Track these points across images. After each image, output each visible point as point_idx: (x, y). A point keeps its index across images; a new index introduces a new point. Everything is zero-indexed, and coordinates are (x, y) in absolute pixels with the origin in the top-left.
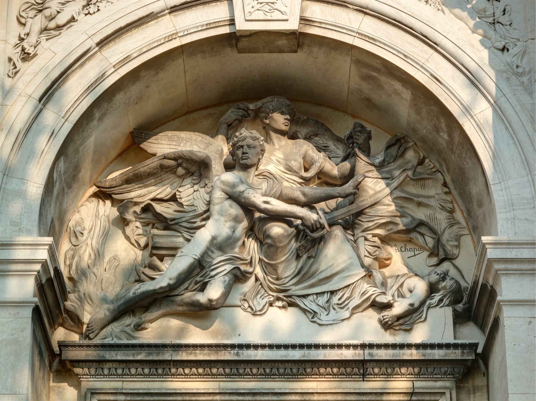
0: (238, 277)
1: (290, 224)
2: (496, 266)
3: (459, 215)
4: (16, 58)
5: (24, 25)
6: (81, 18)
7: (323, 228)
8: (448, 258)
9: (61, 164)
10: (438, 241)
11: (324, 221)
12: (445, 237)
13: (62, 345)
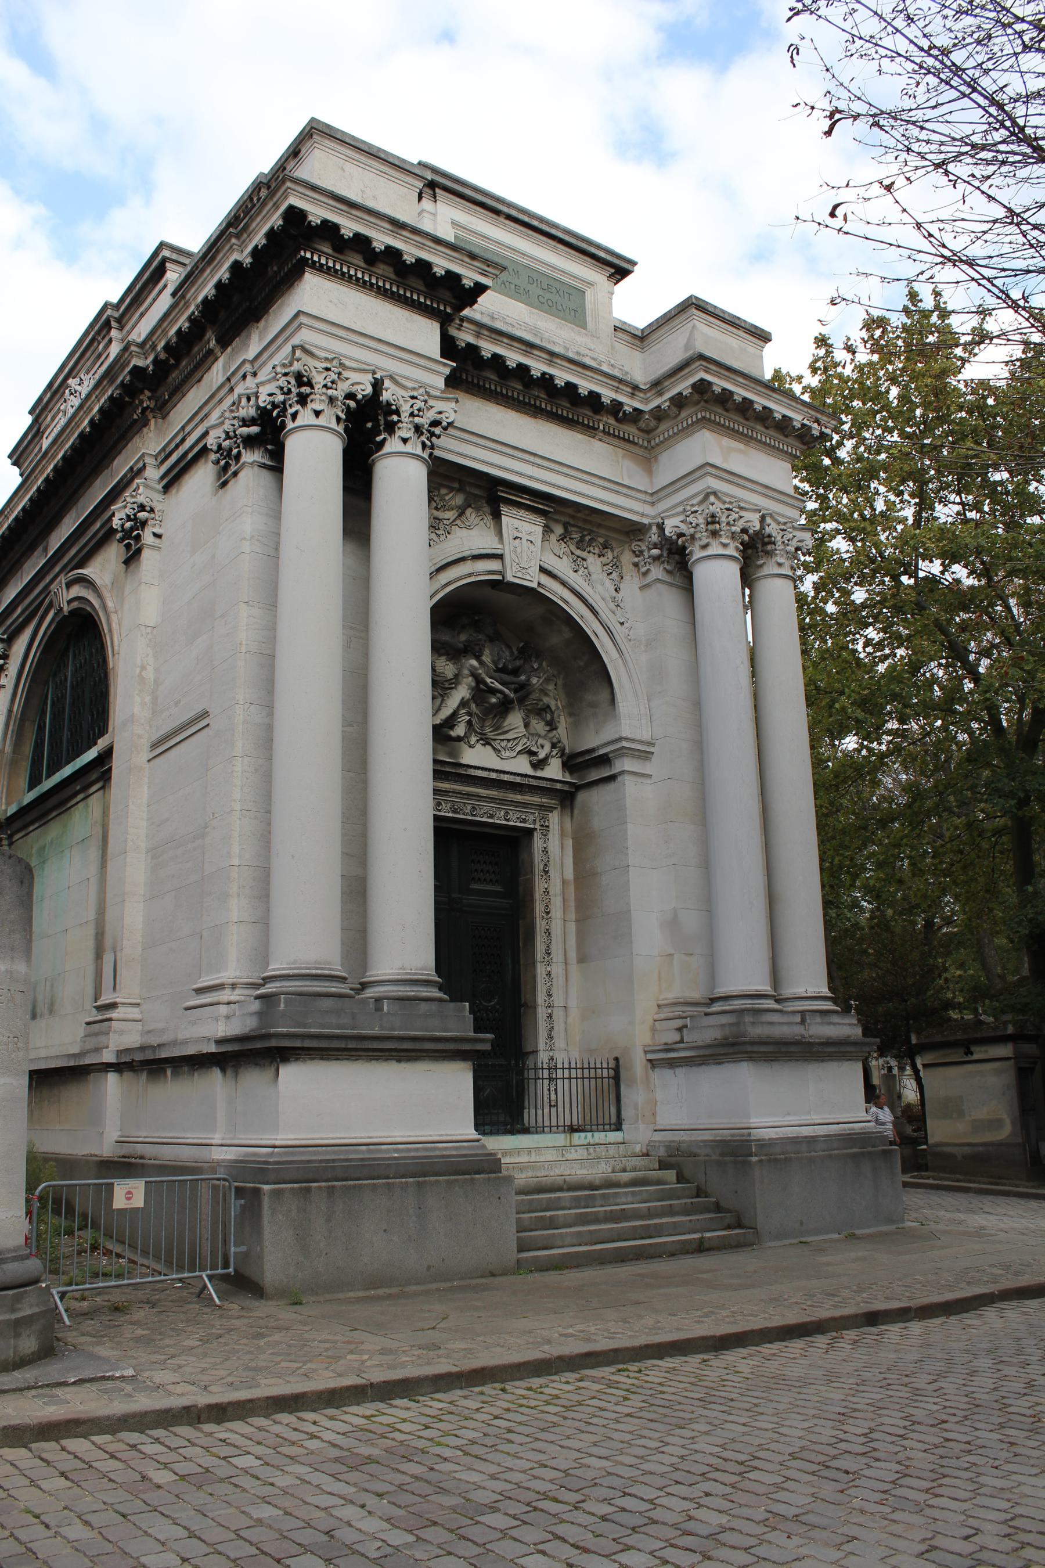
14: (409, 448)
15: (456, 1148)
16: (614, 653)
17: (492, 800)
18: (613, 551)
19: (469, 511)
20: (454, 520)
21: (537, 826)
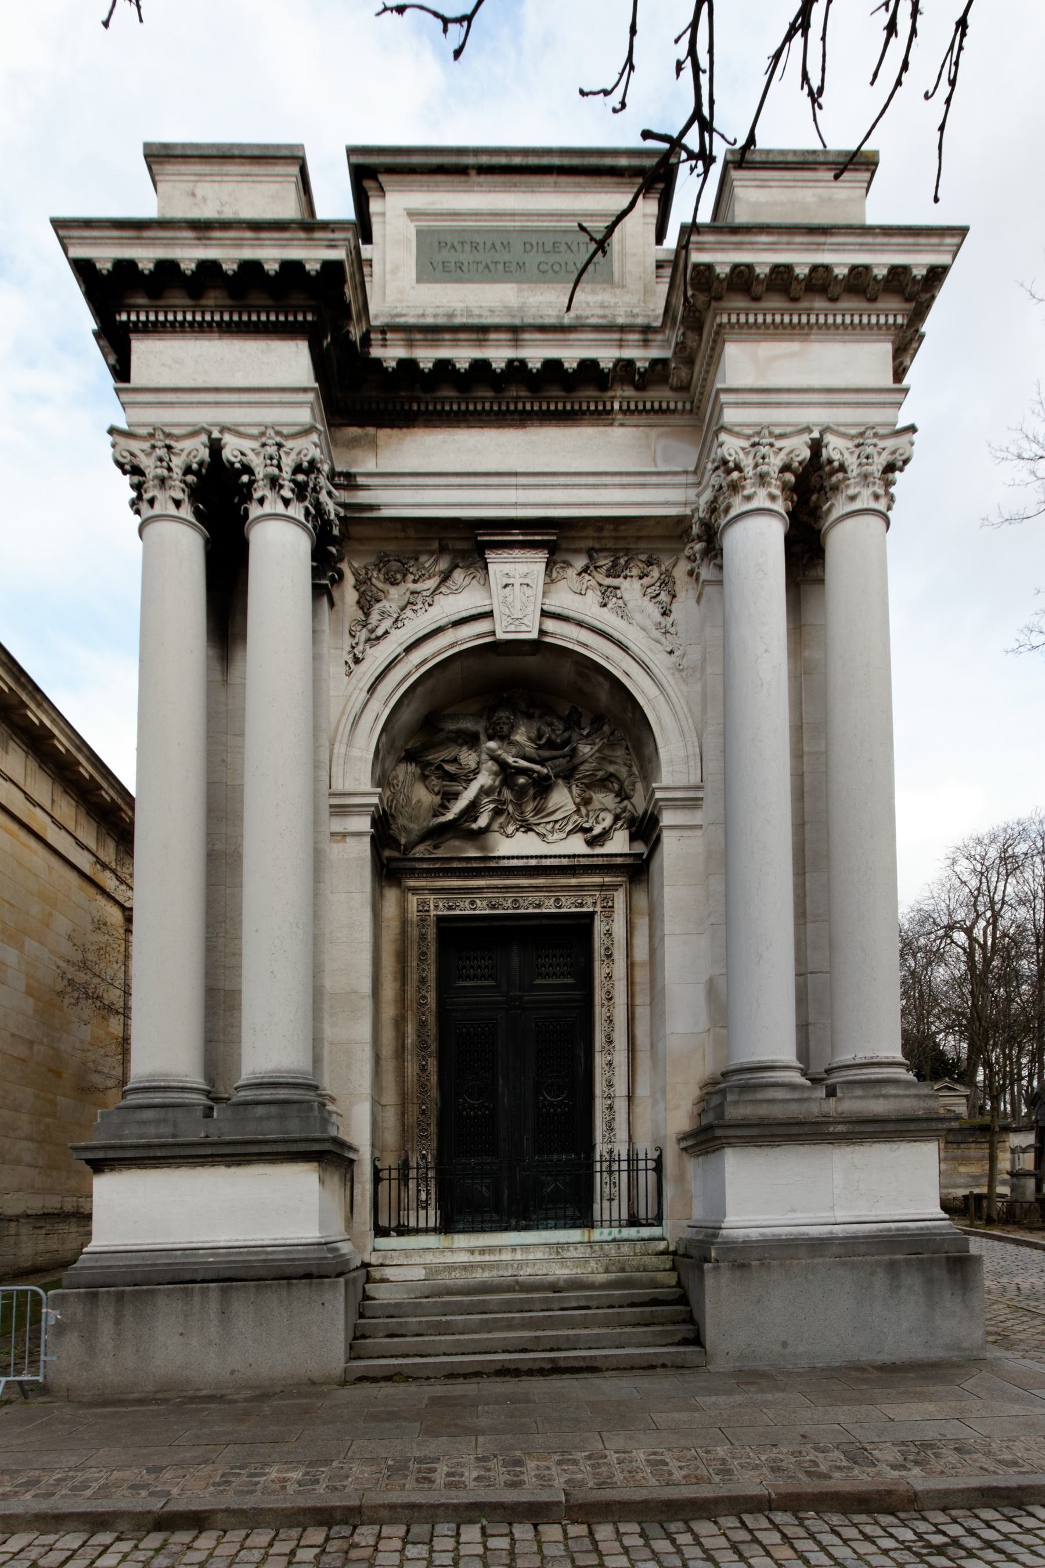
0: (497, 813)
1: (530, 776)
2: (661, 803)
3: (635, 770)
4: (350, 662)
5: (354, 637)
6: (393, 631)
7: (550, 778)
8: (628, 797)
9: (384, 738)
10: (621, 787)
11: (551, 774)
12: (626, 783)
13: (390, 859)
14: (291, 511)
15: (287, 1252)
16: (652, 690)
17: (537, 888)
18: (659, 566)
19: (458, 575)
20: (438, 587)
21: (598, 909)
